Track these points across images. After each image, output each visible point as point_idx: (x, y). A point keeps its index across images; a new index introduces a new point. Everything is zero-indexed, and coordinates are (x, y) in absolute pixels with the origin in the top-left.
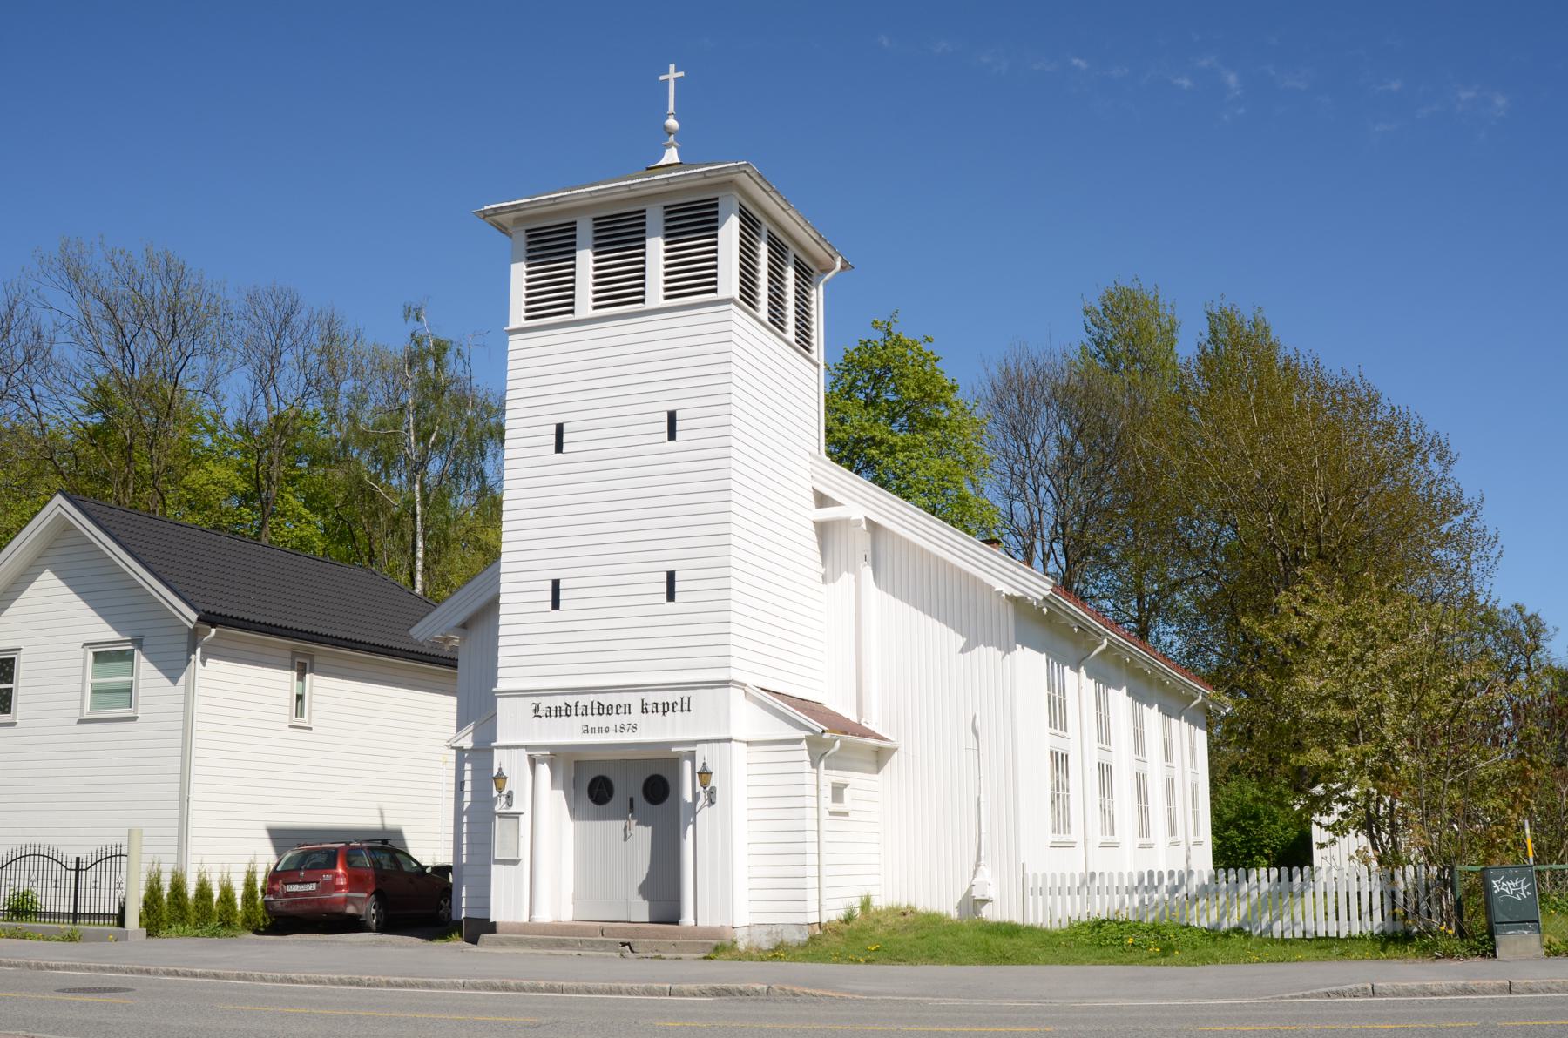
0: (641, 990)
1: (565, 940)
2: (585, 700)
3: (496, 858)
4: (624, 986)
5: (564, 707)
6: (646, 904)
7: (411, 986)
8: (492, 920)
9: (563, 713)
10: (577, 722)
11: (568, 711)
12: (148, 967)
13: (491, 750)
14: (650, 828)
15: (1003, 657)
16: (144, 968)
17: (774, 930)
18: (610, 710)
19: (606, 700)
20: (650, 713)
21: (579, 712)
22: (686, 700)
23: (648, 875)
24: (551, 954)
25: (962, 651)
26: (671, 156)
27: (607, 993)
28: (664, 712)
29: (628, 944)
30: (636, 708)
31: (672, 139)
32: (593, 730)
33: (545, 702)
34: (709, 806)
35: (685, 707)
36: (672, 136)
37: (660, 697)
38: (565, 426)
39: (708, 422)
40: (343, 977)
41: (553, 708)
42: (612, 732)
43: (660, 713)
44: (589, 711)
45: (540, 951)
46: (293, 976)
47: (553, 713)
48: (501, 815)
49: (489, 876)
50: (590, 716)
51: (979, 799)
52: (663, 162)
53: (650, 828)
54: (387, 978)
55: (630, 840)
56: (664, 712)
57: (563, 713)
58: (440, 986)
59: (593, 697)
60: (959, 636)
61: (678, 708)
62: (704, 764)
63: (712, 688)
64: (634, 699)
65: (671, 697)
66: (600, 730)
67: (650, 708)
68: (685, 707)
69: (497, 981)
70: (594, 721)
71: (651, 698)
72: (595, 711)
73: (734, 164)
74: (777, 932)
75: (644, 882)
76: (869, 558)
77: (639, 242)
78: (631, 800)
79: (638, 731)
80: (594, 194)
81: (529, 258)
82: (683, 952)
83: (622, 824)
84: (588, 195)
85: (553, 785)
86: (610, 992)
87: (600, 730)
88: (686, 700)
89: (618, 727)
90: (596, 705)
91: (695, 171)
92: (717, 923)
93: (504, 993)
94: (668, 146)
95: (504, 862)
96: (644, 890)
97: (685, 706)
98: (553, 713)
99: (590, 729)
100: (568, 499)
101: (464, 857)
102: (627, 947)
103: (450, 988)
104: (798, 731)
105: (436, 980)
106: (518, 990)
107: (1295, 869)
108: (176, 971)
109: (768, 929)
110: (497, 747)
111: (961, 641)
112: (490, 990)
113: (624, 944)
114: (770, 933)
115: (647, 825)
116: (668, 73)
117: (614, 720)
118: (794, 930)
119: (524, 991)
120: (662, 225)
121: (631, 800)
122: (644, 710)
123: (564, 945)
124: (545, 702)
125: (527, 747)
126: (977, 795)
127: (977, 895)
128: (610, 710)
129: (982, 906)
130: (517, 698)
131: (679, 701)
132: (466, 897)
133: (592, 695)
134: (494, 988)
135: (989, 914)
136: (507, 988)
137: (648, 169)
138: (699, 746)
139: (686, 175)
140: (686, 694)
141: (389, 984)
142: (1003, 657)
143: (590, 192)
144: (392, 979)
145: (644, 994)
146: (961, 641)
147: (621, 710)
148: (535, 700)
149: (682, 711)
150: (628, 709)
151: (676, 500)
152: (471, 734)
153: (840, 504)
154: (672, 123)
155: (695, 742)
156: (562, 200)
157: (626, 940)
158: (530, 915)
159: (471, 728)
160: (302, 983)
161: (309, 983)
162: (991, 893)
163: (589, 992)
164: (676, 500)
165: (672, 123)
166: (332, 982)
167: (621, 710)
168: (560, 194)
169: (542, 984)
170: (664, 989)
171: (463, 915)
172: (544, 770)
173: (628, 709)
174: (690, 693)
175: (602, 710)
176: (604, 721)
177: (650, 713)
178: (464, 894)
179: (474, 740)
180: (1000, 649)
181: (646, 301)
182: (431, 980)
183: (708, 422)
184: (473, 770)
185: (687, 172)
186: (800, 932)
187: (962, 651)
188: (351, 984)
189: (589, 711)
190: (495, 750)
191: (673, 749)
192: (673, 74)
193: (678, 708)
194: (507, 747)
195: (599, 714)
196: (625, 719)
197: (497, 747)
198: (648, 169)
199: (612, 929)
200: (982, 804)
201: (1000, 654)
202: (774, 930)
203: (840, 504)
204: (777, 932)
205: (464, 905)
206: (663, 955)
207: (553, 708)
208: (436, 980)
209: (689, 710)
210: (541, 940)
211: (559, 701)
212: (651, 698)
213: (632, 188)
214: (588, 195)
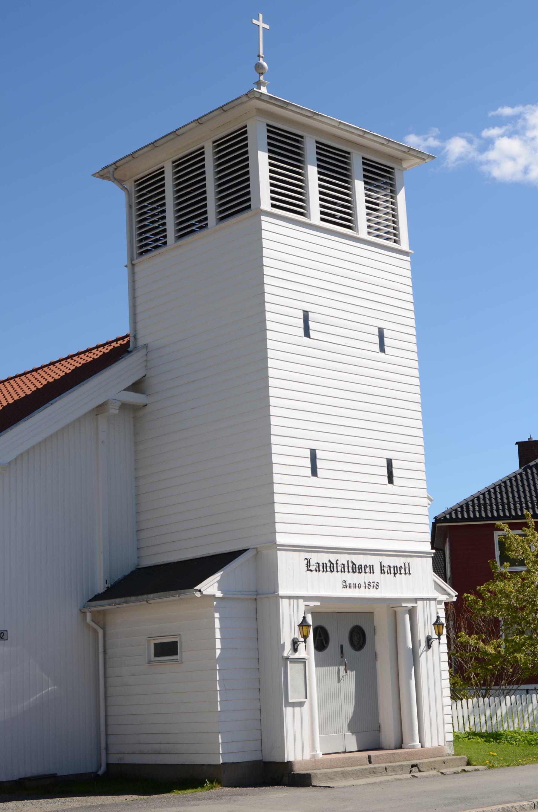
1: (375, 768)
2: (343, 559)
3: (290, 700)
5: (328, 564)
10: (338, 577)
19: (360, 560)
21: (339, 569)
23: (355, 712)
28: (395, 574)
30: (377, 569)
33: (315, 558)
43: (392, 575)
50: (346, 573)
55: (342, 682)
56: (395, 574)
61: (403, 571)
63: (421, 557)
64: (374, 561)
65: (398, 562)
67: (386, 569)
72: (350, 570)
75: (352, 718)
78: (342, 647)
83: (336, 668)
88: (407, 565)
90: (351, 565)
92: (435, 744)
99: (347, 584)
121: (342, 647)
122: (382, 571)
124: (315, 558)
125: (306, 598)
131: (403, 567)
133: (347, 555)
138: (419, 602)
147: (368, 570)
148: (308, 555)
149: (406, 574)
152: (216, 585)
155: (416, 600)
157: (414, 762)
159: (219, 578)
167: (368, 570)
175: (357, 569)
195: (359, 572)
207: (321, 565)
209: (410, 574)
211: (324, 558)
212: (388, 561)
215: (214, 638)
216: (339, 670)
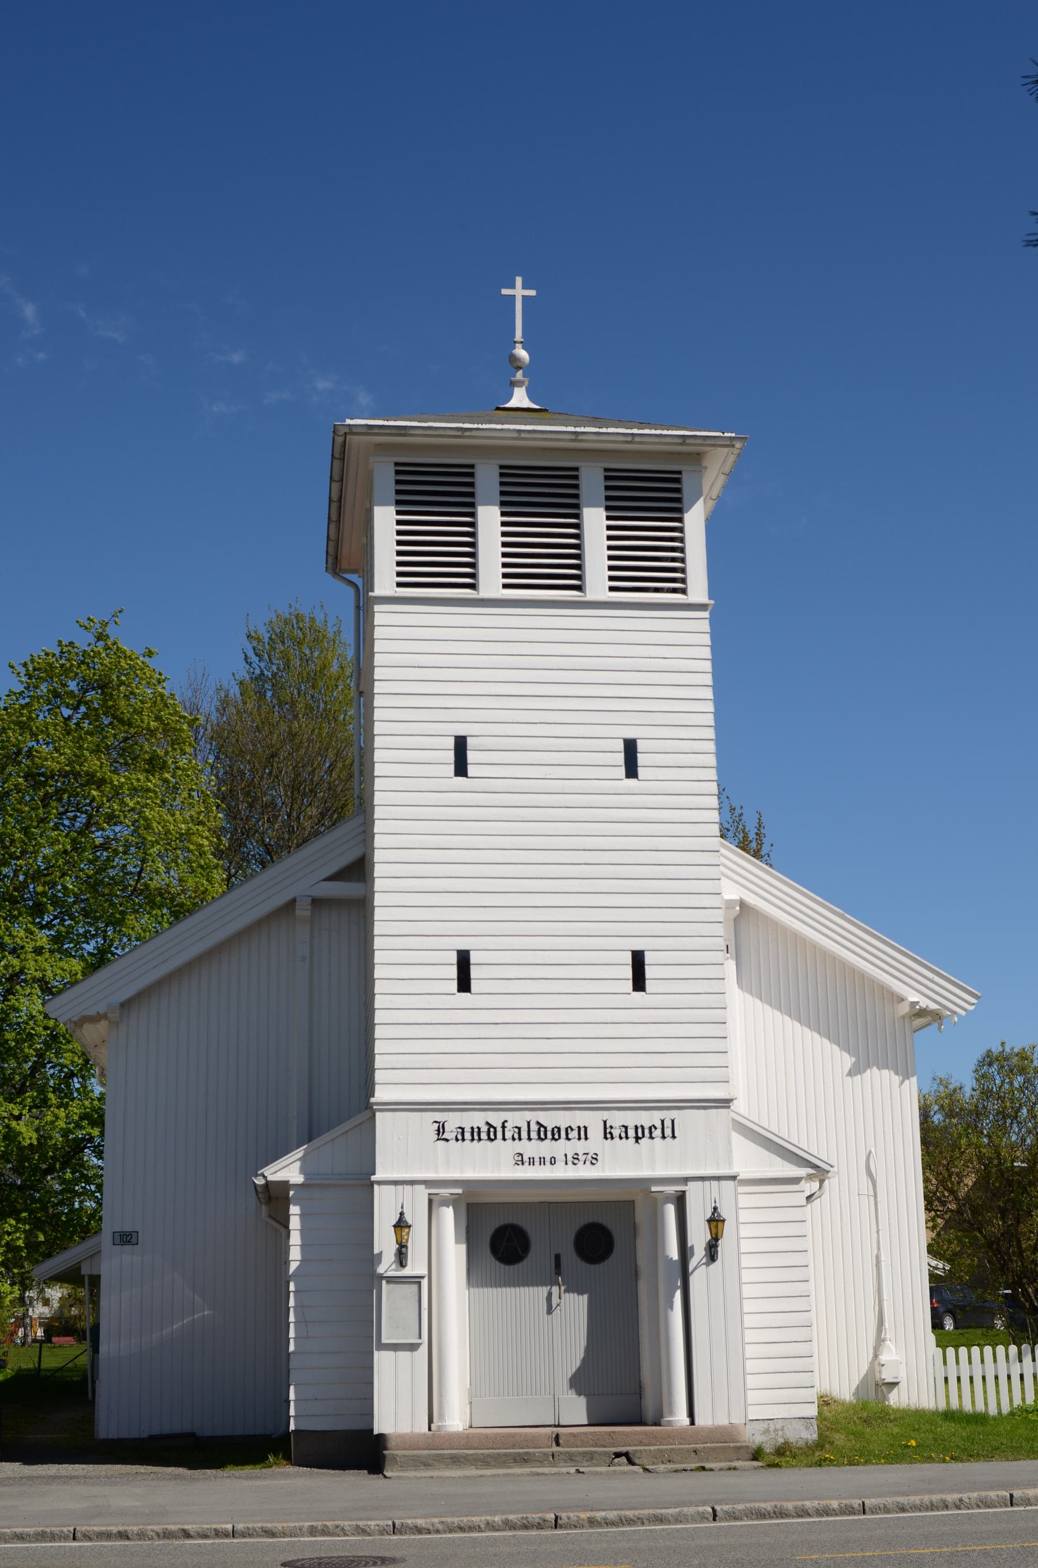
0: (973, 1501)
1: (527, 1453)
2: (517, 1119)
3: (384, 1340)
4: (950, 1498)
5: (484, 1128)
6: (582, 1401)
7: (630, 1522)
8: (376, 1432)
9: (484, 1136)
10: (506, 1149)
11: (492, 1133)
12: (121, 1528)
13: (372, 1184)
14: (586, 1296)
15: (902, 1083)
16: (114, 1529)
17: (772, 1428)
18: (556, 1134)
19: (551, 1119)
20: (617, 1139)
21: (508, 1135)
22: (668, 1124)
23: (584, 1361)
24: (538, 1474)
25: (850, 1074)
26: (520, 399)
27: (927, 1509)
28: (637, 1139)
29: (626, 1455)
30: (596, 1132)
31: (519, 375)
32: (532, 1161)
33: (453, 1121)
34: (707, 1264)
35: (668, 1132)
36: (520, 372)
37: (632, 1119)
38: (470, 741)
39: (683, 759)
40: (511, 1517)
41: (468, 1130)
42: (560, 1163)
43: (632, 1140)
44: (524, 1135)
45: (488, 1472)
46: (421, 1522)
47: (468, 1136)
48: (391, 1280)
49: (371, 1368)
50: (525, 1141)
51: (878, 1257)
52: (508, 405)
53: (586, 1296)
54: (589, 1514)
55: (556, 1313)
56: (637, 1139)
57: (484, 1136)
58: (677, 1520)
59: (529, 1115)
60: (846, 1055)
61: (657, 1133)
62: (715, 1209)
63: (705, 1108)
64: (593, 1120)
65: (646, 1118)
66: (542, 1161)
67: (616, 1132)
68: (668, 1132)
69: (768, 1506)
70: (532, 1148)
71: (617, 1119)
72: (534, 1135)
73: (720, 434)
74: (776, 1430)
75: (579, 1370)
76: (732, 949)
77: (468, 507)
78: (558, 1257)
79: (599, 1164)
80: (523, 435)
81: (398, 503)
82: (708, 1460)
83: (543, 1291)
84: (680, 441)
85: (457, 1242)
86: (932, 1507)
87: (542, 1161)
88: (668, 1124)
89: (570, 1158)
90: (534, 1127)
91: (653, 432)
92: (723, 1421)
93: (628, 1529)
94: (513, 384)
95: (395, 1347)
96: (579, 1382)
97: (669, 1132)
98: (468, 1136)
99: (526, 1159)
100: (479, 842)
101: (292, 1342)
102: (624, 1459)
103: (694, 1521)
104: (794, 1168)
105: (670, 1511)
106: (799, 1516)
107: (1025, 1347)
108: (184, 1530)
109: (765, 1425)
110: (379, 1183)
111: (848, 1061)
112: (757, 1518)
113: (618, 1455)
114: (767, 1431)
115: (580, 1292)
116: (524, 287)
117: (561, 1148)
118: (799, 1426)
119: (809, 1515)
120: (392, 487)
121: (558, 1257)
122: (608, 1134)
123: (526, 1461)
124: (453, 1121)
125: (427, 1183)
126: (875, 1252)
127: (888, 1376)
128: (556, 1134)
129: (890, 1391)
130: (561, 1112)
131: (659, 1125)
132: (295, 1401)
133: (527, 1113)
134: (762, 1515)
135: (896, 1399)
136: (782, 1514)
137: (498, 409)
138: (690, 1184)
139: (661, 435)
140: (668, 1115)
141: (592, 1522)
142: (902, 1083)
143: (519, 431)
144: (599, 1515)
145: (978, 1507)
146: (848, 1061)
147: (573, 1134)
148: (439, 1117)
149: (664, 1137)
150: (583, 1133)
151: (642, 857)
152: (298, 1164)
153: (326, 880)
154: (522, 353)
155: (686, 1180)
156: (474, 433)
157: (624, 1449)
158: (431, 1421)
159: (301, 1155)
160: (438, 1531)
161: (451, 1531)
162: (902, 1376)
163: (903, 1510)
164: (642, 857)
165: (522, 353)
166: (491, 1527)
167: (573, 1134)
168: (475, 426)
169: (835, 1504)
170: (226, 1530)
171: (292, 1427)
172: (448, 1215)
173: (583, 1133)
174: (674, 1114)
175: (543, 1133)
176: (547, 1149)
177: (617, 1139)
178: (292, 1396)
179: (303, 1171)
180: (897, 1073)
181: (689, 591)
182: (663, 1511)
183: (683, 759)
184: (303, 1216)
185: (665, 432)
186: (807, 1428)
187: (850, 1074)
188: (526, 1527)
189: (524, 1135)
190: (376, 1187)
191: (653, 1189)
192: (519, 291)
193: (657, 1133)
194: (395, 1183)
196: (579, 1147)
197: (379, 1183)
198: (498, 409)
199: (574, 1435)
200: (883, 1265)
201: (897, 1079)
202: (772, 1428)
203: (326, 880)
204: (776, 1430)
205: (292, 1412)
206: (708, 1465)
207: (468, 1130)
208: (670, 1511)
209: (674, 1137)
210: (489, 1456)
211: (477, 1119)
212: (617, 1119)
213: (580, 437)
214: (516, 435)
215: (304, 1246)
216: (550, 1294)
